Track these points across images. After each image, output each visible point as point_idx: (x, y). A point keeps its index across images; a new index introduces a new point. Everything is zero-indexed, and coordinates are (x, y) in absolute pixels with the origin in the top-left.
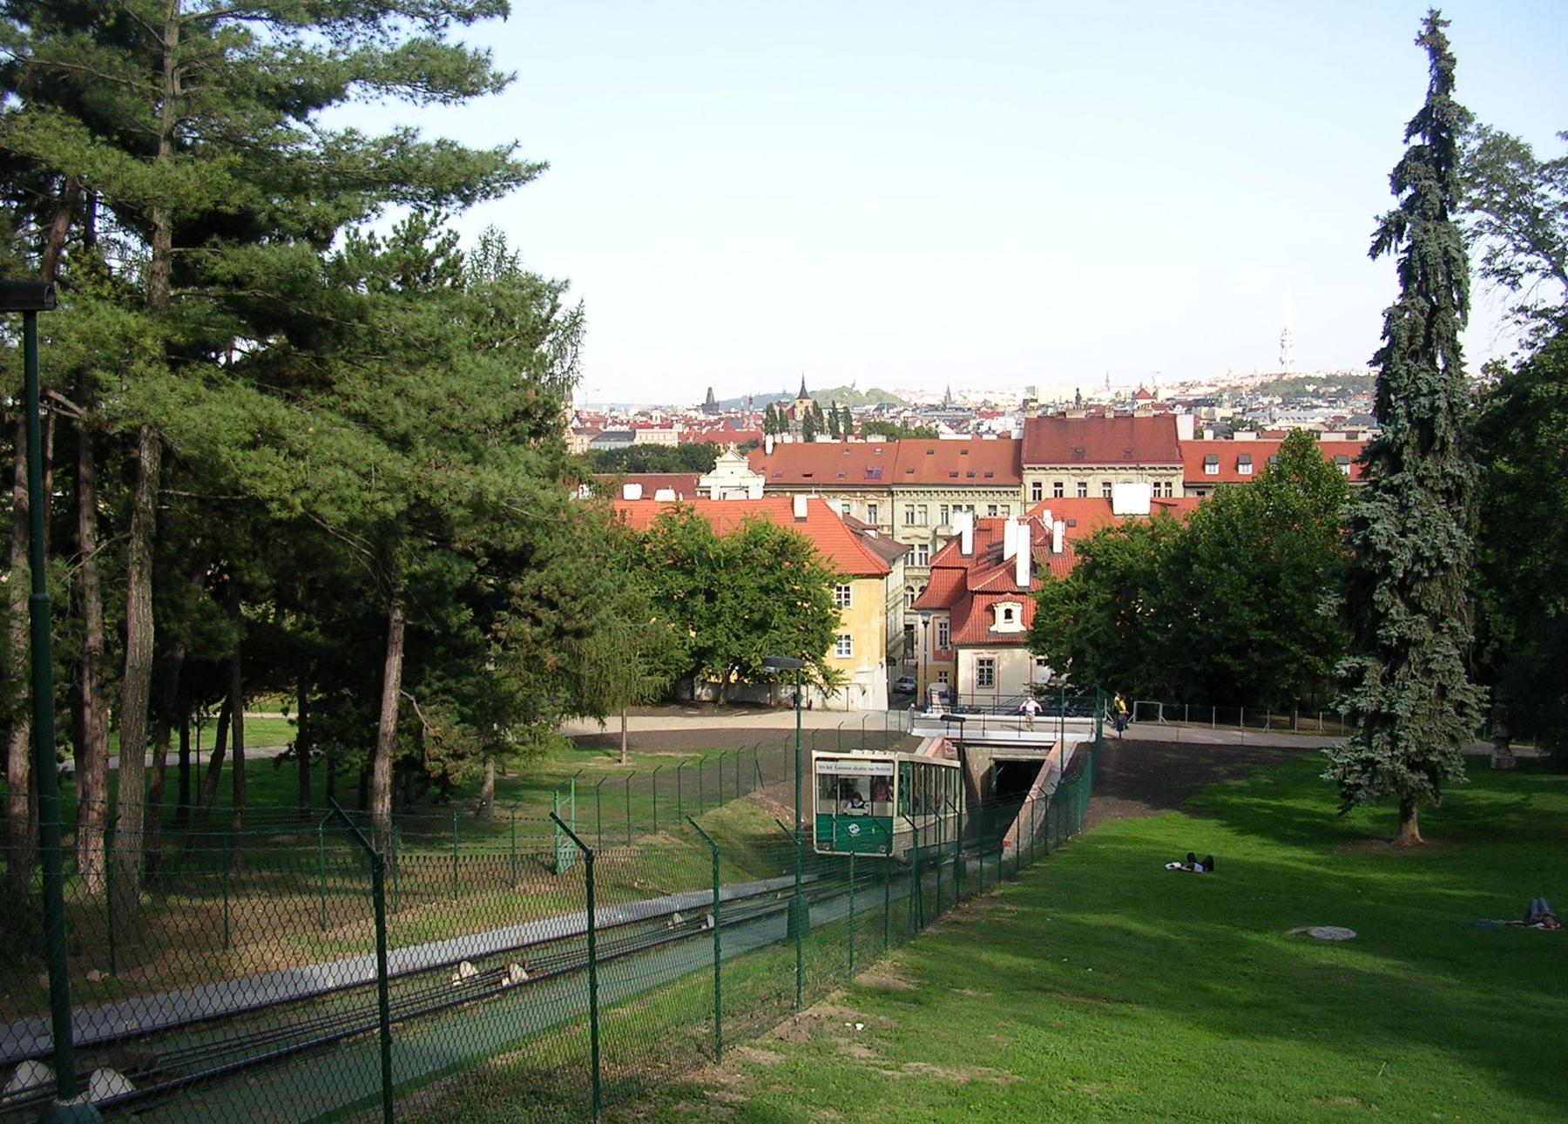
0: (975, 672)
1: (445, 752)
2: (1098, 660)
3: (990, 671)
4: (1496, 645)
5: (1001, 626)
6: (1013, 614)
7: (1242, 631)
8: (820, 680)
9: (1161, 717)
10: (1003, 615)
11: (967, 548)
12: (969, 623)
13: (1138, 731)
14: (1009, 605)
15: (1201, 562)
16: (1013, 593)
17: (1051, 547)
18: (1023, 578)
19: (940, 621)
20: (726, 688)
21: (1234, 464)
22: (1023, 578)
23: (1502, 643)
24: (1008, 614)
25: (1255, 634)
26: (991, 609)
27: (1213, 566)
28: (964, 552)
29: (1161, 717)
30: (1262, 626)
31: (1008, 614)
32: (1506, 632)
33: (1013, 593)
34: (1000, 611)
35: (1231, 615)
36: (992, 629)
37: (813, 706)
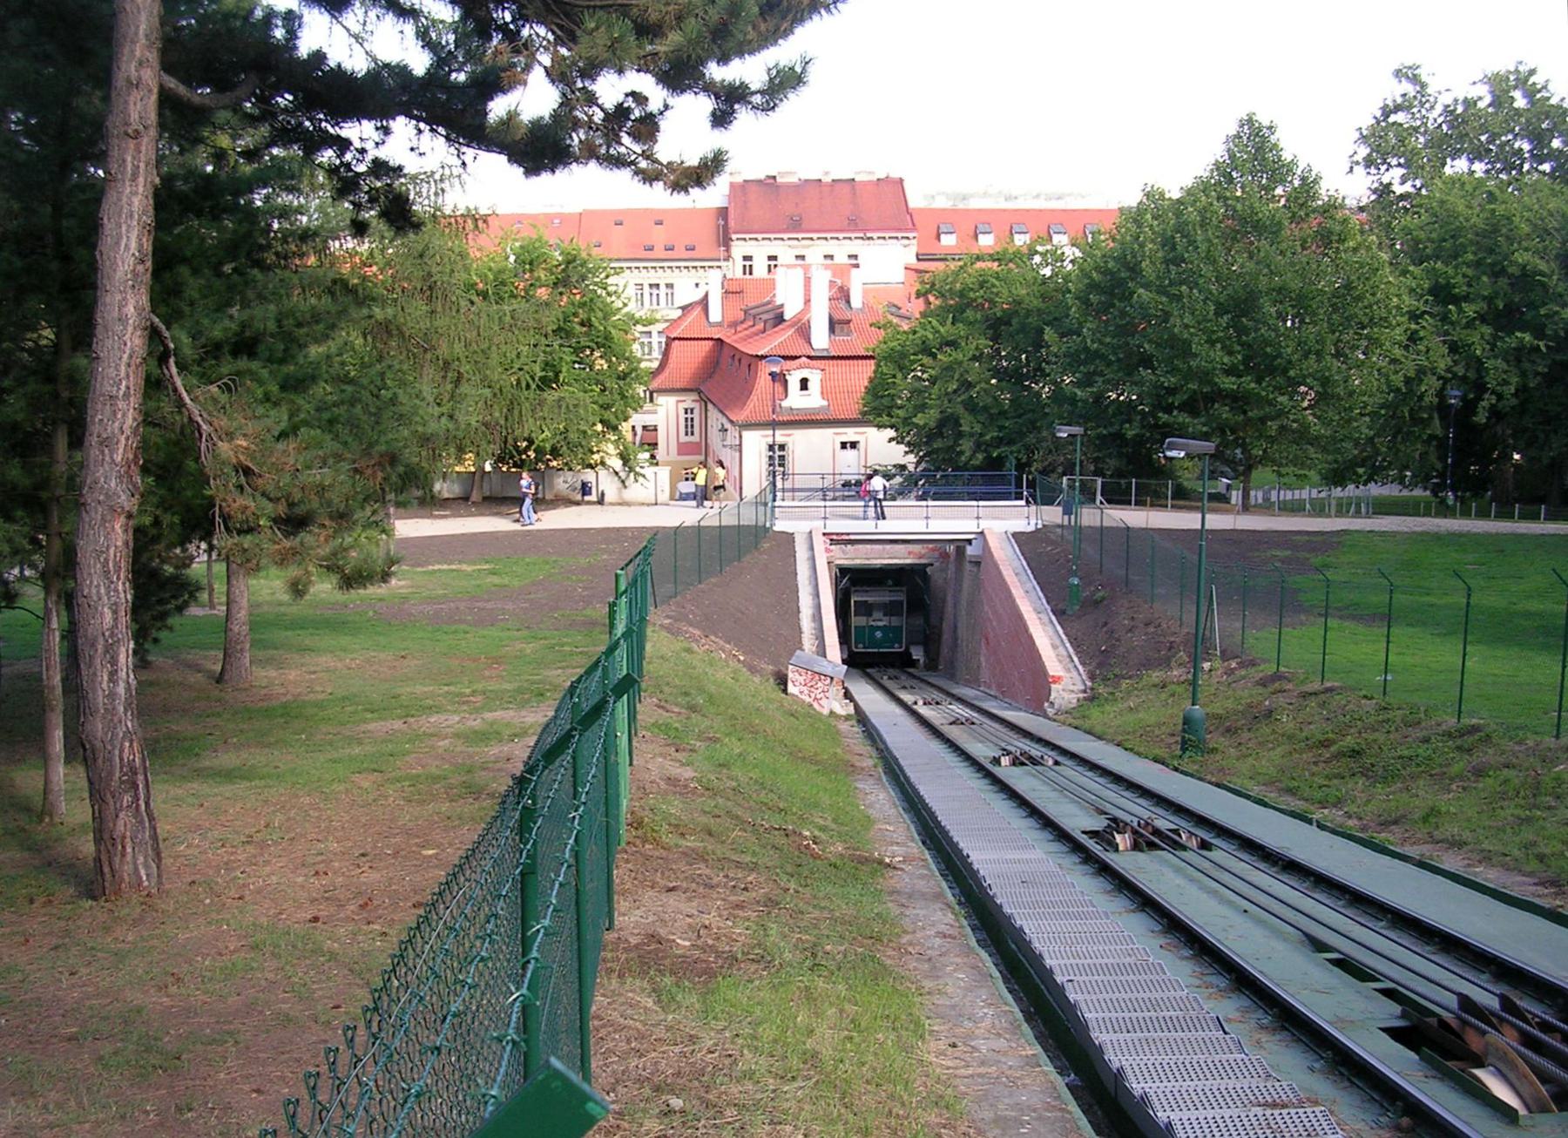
0: (765, 460)
1: (269, 507)
2: (978, 428)
3: (782, 458)
4: (1494, 400)
5: (796, 400)
6: (810, 385)
7: (1205, 377)
8: (616, 463)
9: (1099, 497)
10: (798, 385)
11: (715, 314)
12: (754, 397)
13: (1089, 516)
14: (805, 373)
15: (1146, 286)
16: (809, 357)
17: (848, 302)
18: (821, 339)
19: (686, 405)
20: (482, 477)
21: (972, 233)
22: (821, 339)
23: (1500, 397)
24: (804, 384)
25: (1228, 383)
26: (780, 379)
27: (1162, 291)
28: (711, 320)
29: (1099, 497)
30: (1230, 371)
31: (804, 384)
32: (1506, 383)
33: (809, 357)
34: (794, 381)
35: (1196, 355)
36: (785, 404)
37: (607, 499)
